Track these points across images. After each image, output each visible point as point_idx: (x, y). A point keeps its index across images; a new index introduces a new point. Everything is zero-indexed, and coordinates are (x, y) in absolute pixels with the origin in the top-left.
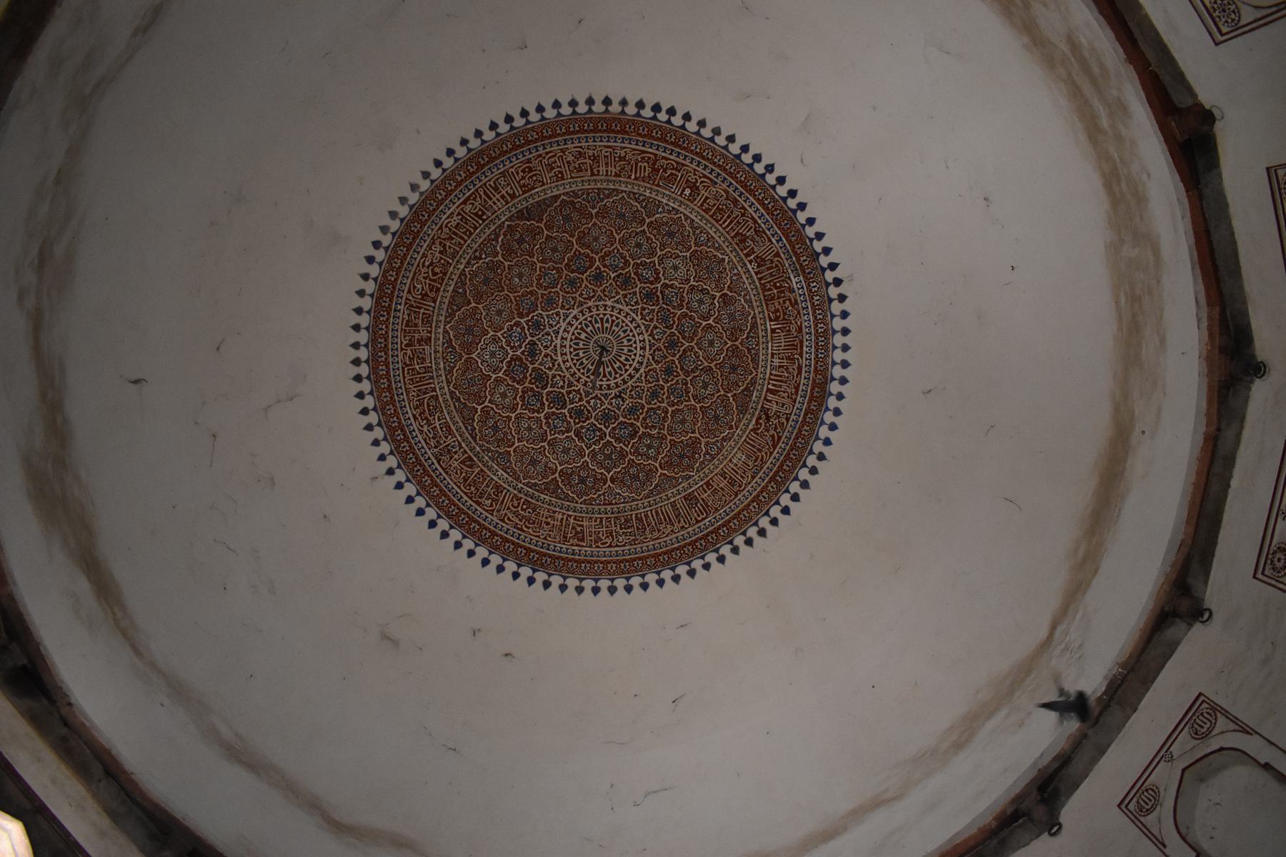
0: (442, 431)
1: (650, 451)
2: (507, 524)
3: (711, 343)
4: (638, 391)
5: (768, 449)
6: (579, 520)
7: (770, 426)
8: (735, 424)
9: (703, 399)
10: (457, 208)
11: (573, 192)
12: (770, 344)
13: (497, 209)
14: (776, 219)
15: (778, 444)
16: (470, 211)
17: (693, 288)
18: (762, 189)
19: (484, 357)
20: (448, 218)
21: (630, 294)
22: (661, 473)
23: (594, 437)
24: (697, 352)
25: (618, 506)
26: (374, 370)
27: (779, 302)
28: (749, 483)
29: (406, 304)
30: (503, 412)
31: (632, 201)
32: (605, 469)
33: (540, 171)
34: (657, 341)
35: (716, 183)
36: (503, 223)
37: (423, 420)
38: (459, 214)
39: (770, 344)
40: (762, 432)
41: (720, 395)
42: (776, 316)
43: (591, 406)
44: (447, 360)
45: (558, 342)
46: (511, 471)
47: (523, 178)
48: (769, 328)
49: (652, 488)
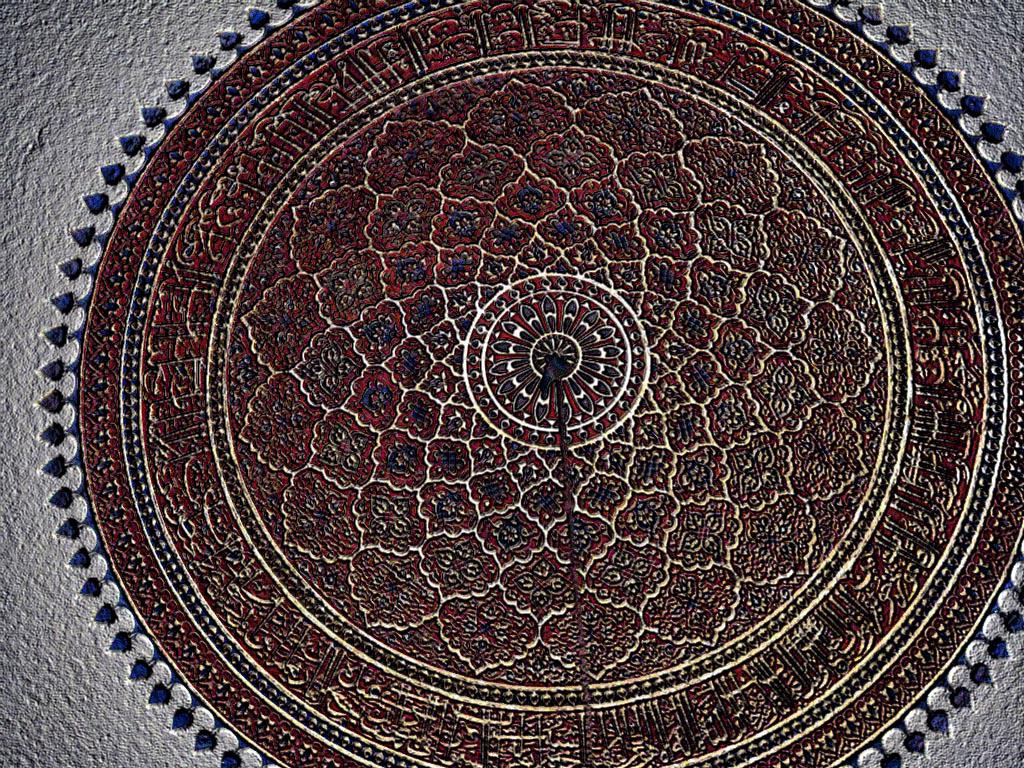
0: (214, 522)
1: (628, 583)
2: (329, 715)
3: (782, 392)
4: (617, 456)
5: (871, 629)
6: (472, 714)
7: (883, 583)
8: (810, 560)
9: (750, 494)
10: (288, 96)
11: (539, 74)
12: (907, 422)
13: (371, 97)
14: (968, 200)
15: (894, 623)
16: (314, 103)
17: (758, 278)
18: (947, 138)
19: (312, 374)
20: (267, 114)
21: (625, 266)
22: (646, 631)
23: (517, 540)
24: (750, 402)
25: (553, 689)
26: (87, 415)
27: (941, 354)
28: (824, 689)
29: (163, 277)
30: (341, 483)
31: (659, 104)
32: (533, 607)
33: (472, 32)
34: (668, 364)
35: (850, 107)
36: (381, 123)
37: (177, 505)
38: (291, 107)
39: (907, 422)
40: (863, 590)
41: (787, 496)
42: (930, 373)
43: (517, 475)
44: (238, 382)
45: (466, 343)
46: (345, 603)
47: (435, 44)
48: (910, 395)
49: (623, 660)
